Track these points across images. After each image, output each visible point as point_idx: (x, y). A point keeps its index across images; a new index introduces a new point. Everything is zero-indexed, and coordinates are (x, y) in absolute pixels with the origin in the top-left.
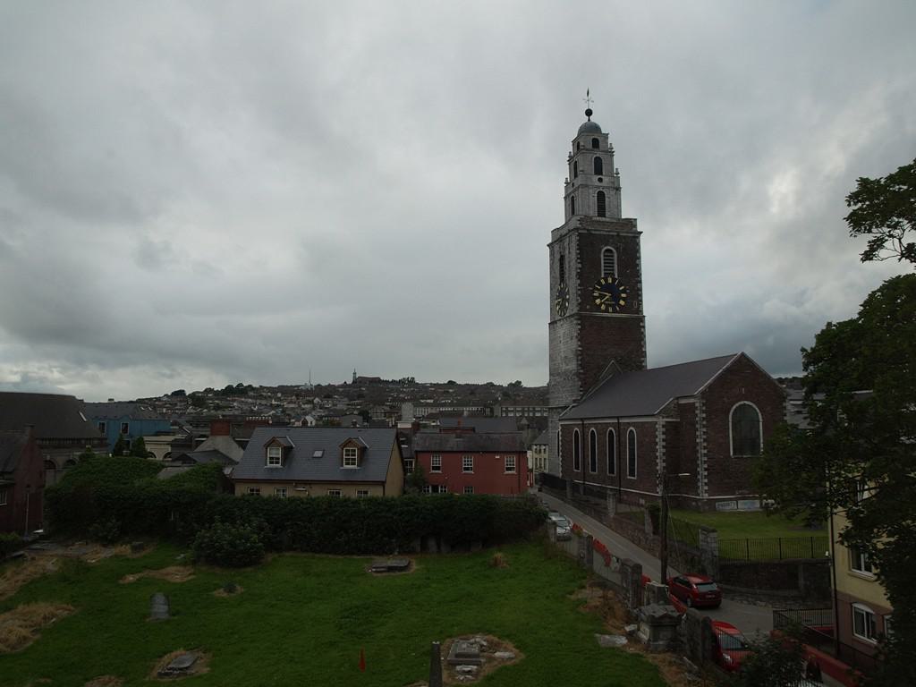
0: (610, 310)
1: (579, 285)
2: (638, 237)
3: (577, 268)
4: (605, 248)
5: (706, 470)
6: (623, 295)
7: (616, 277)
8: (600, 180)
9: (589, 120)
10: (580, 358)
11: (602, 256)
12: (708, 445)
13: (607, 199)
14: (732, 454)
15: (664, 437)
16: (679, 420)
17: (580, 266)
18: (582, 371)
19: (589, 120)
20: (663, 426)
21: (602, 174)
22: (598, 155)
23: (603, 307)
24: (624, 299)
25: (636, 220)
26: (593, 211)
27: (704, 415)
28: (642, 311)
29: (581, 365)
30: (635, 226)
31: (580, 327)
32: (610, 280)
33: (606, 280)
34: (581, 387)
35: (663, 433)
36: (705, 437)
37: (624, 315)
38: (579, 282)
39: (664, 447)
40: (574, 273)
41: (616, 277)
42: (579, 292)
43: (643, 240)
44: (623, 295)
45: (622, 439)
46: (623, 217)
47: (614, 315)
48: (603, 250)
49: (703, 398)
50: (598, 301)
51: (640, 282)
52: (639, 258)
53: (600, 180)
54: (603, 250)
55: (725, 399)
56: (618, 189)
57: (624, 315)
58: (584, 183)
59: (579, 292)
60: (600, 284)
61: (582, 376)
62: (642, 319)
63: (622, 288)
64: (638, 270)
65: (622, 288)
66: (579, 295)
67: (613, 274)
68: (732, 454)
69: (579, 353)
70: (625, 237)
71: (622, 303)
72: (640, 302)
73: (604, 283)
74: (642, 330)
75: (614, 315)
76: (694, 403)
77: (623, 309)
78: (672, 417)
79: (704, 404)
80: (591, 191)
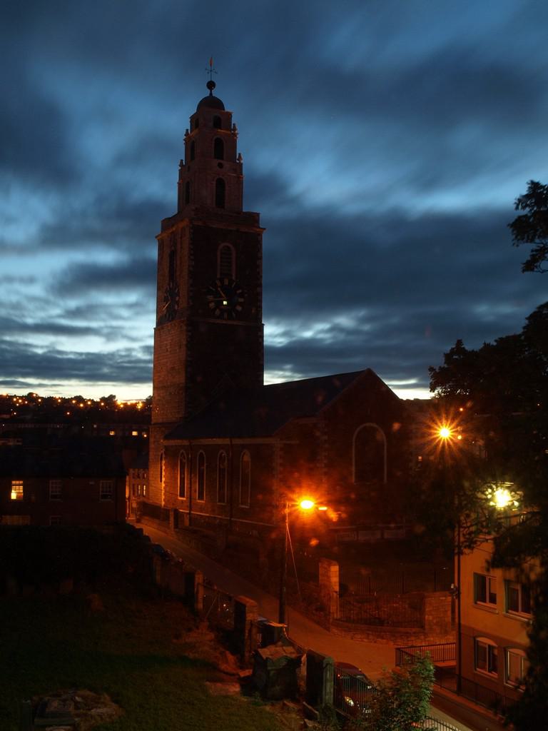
0: (226, 316)
6: (241, 300)
7: (234, 278)
9: (211, 94)
11: (219, 253)
19: (211, 94)
24: (241, 304)
31: (190, 334)
32: (226, 282)
41: (234, 278)
44: (241, 300)
46: (244, 211)
47: (230, 322)
53: (221, 165)
63: (240, 291)
65: (240, 291)
71: (239, 308)
73: (218, 283)
75: (230, 322)
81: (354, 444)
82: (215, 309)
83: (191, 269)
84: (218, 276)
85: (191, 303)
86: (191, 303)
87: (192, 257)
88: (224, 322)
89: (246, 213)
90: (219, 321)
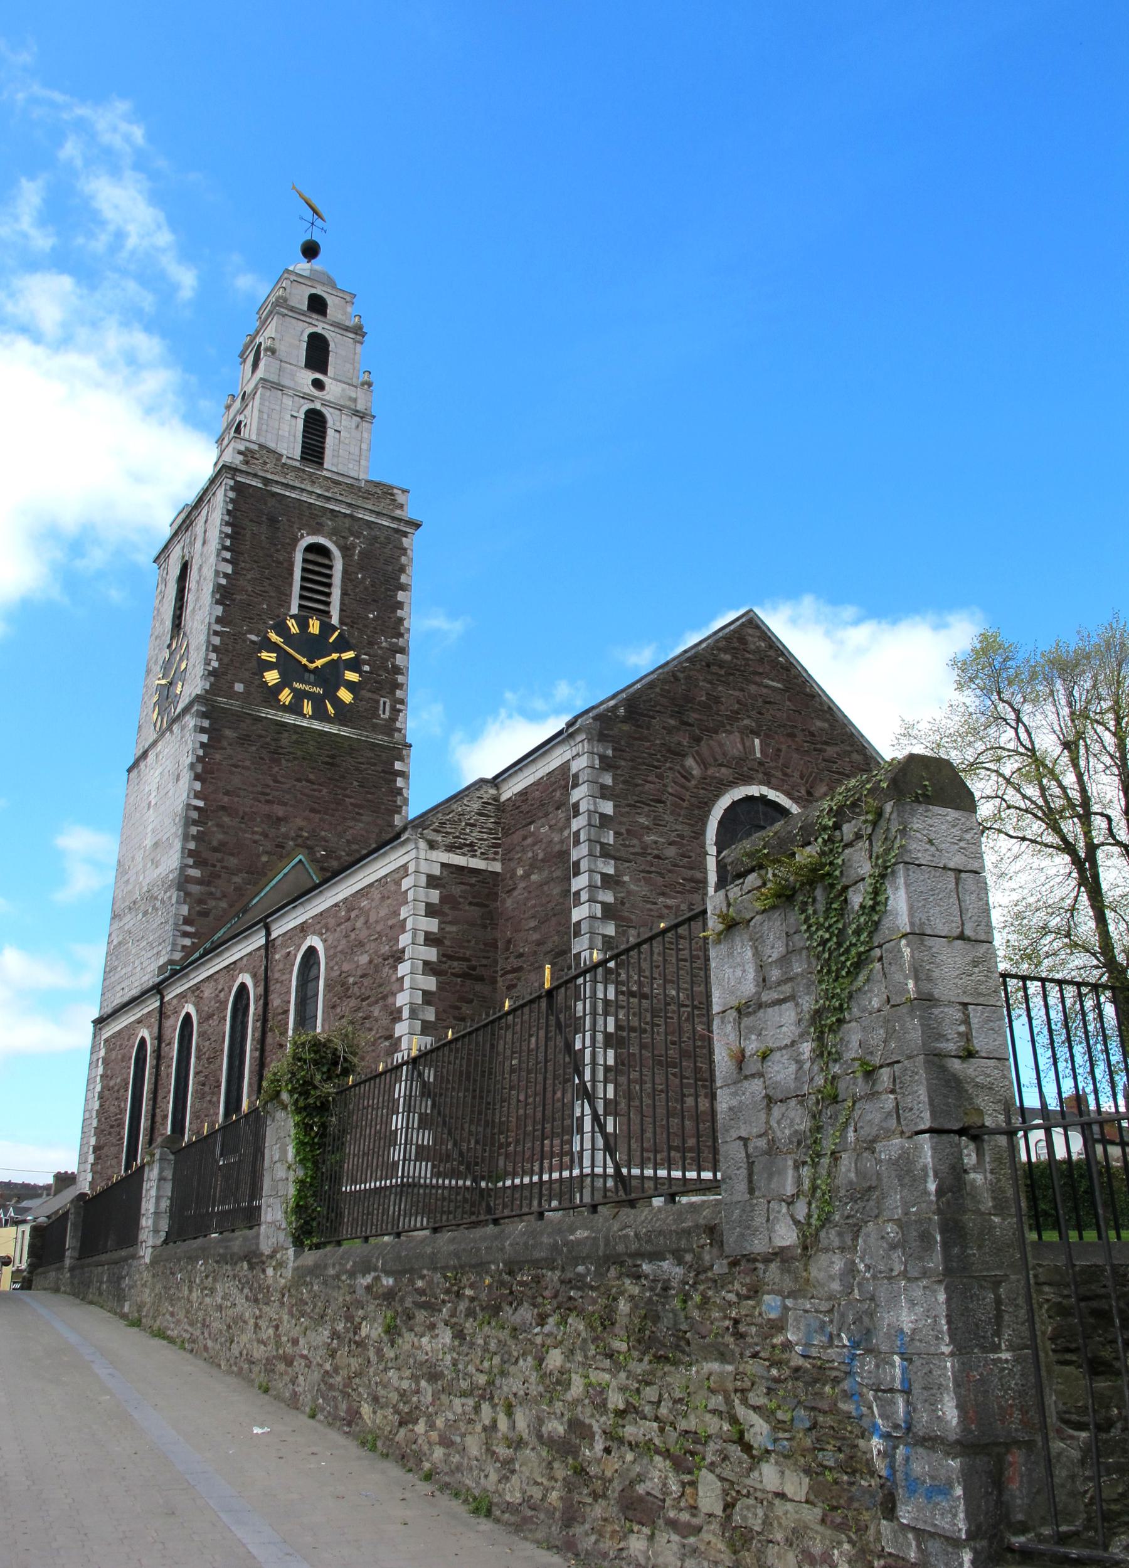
0: (308, 708)
1: (219, 620)
3: (217, 573)
5: (610, 1041)
6: (352, 676)
7: (335, 621)
10: (194, 830)
11: (299, 557)
13: (330, 433)
15: (432, 925)
16: (497, 867)
18: (195, 873)
20: (432, 882)
21: (324, 371)
22: (319, 330)
23: (286, 696)
24: (351, 686)
26: (290, 444)
27: (607, 807)
29: (191, 853)
31: (204, 738)
32: (314, 627)
33: (303, 624)
34: (187, 921)
35: (431, 911)
36: (608, 897)
37: (345, 732)
38: (219, 610)
39: (429, 968)
40: (208, 588)
41: (335, 621)
42: (217, 641)
43: (415, 543)
45: (276, 1002)
47: (317, 725)
49: (602, 737)
50: (272, 677)
51: (403, 651)
53: (318, 384)
55: (690, 762)
57: (345, 732)
58: (273, 378)
59: (217, 641)
60: (282, 630)
61: (195, 889)
62: (400, 750)
64: (401, 620)
66: (215, 649)
67: (327, 613)
69: (195, 815)
71: (345, 695)
73: (294, 629)
74: (400, 782)
75: (317, 725)
76: (565, 766)
77: (344, 714)
78: (470, 849)
79: (606, 764)
80: (288, 402)
81: (712, 850)
82: (278, 688)
83: (223, 582)
84: (294, 610)
85: (215, 664)
86: (215, 664)
87: (228, 555)
88: (305, 723)
89: (377, 484)
90: (289, 719)
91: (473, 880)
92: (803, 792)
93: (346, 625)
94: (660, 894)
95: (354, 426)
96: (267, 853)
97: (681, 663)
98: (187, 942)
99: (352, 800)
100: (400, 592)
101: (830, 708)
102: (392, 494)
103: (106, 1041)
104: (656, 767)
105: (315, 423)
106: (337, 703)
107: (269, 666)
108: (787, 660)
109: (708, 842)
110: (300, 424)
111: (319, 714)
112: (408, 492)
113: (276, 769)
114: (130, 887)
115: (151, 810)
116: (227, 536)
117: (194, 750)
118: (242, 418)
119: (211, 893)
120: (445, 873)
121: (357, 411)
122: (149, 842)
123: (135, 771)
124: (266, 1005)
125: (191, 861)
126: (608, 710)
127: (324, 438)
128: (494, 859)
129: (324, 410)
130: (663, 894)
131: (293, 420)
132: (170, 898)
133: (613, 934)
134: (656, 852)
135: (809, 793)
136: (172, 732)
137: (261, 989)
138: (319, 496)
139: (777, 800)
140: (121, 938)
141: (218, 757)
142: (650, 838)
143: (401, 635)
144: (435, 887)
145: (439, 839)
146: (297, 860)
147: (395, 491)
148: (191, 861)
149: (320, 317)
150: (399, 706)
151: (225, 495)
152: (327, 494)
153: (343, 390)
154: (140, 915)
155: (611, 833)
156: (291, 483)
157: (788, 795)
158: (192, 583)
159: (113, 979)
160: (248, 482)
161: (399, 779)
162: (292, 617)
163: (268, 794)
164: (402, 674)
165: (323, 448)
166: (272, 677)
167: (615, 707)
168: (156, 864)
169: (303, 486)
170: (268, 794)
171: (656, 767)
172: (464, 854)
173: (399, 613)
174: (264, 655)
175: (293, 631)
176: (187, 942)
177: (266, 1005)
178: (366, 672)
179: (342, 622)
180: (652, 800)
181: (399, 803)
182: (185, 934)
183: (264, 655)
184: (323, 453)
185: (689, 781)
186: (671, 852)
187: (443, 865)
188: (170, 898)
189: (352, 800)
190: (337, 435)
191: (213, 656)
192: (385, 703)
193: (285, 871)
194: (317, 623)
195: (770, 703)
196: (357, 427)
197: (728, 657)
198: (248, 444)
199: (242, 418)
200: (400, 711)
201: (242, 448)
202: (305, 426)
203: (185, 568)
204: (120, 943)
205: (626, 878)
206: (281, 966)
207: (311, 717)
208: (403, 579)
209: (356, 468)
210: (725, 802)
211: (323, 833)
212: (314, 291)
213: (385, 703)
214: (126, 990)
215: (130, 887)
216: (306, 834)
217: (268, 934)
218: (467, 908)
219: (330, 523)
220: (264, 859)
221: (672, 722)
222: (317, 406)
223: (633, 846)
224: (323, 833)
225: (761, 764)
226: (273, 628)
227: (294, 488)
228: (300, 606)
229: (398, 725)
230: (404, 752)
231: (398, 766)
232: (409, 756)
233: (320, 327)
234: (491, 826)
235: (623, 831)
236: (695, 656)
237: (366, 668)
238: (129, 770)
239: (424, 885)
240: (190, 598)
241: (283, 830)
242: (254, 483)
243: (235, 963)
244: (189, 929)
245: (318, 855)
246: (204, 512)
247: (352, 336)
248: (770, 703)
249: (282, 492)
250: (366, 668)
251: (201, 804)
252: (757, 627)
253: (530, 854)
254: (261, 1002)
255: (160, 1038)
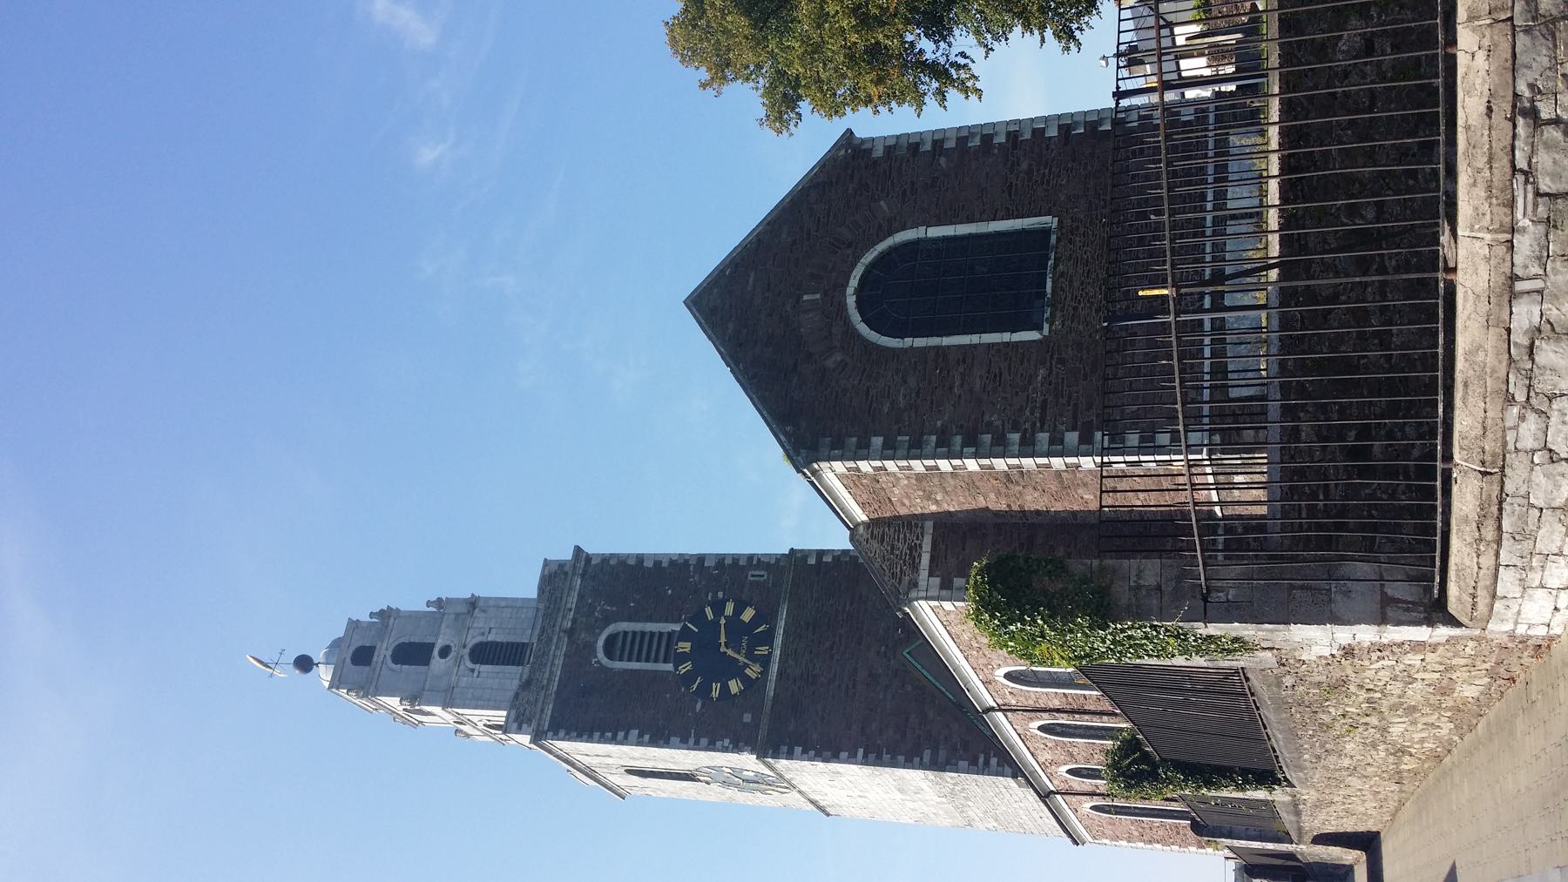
2: (589, 558)
4: (601, 655)
6: (729, 609)
7: (677, 627)
8: (445, 652)
12: (989, 428)
13: (491, 638)
14: (1033, 335)
17: (634, 733)
18: (927, 755)
23: (753, 671)
24: (738, 611)
25: (546, 563)
28: (780, 558)
30: (561, 565)
32: (685, 647)
41: (677, 627)
42: (704, 741)
44: (729, 609)
47: (778, 641)
48: (605, 661)
51: (701, 558)
52: (640, 558)
53: (445, 652)
54: (605, 661)
55: (830, 363)
56: (473, 603)
60: (688, 679)
61: (942, 754)
62: (796, 558)
67: (671, 634)
68: (1033, 335)
70: (581, 597)
71: (748, 615)
72: (754, 562)
73: (686, 667)
75: (778, 641)
78: (915, 549)
82: (746, 680)
83: (647, 737)
84: (670, 667)
85: (726, 742)
86: (726, 742)
87: (621, 735)
88: (777, 652)
89: (541, 590)
91: (942, 547)
92: (849, 251)
93: (681, 617)
94: (951, 392)
95: (483, 615)
96: (903, 686)
97: (740, 370)
98: (994, 761)
99: (848, 605)
100: (645, 564)
101: (768, 224)
102: (550, 576)
103: (1094, 838)
104: (837, 395)
105: (485, 653)
106: (755, 621)
107: (725, 689)
108: (726, 267)
109: (901, 345)
110: (485, 668)
111: (768, 638)
112: (546, 560)
113: (823, 679)
114: (941, 812)
115: (867, 795)
116: (602, 736)
117: (810, 760)
118: (480, 725)
119: (946, 738)
120: (937, 573)
121: (469, 612)
122: (899, 796)
123: (828, 809)
124: (1058, 711)
125: (917, 760)
126: (789, 441)
127: (497, 643)
128: (922, 527)
129: (470, 646)
130: (951, 388)
131: (483, 675)
132: (951, 778)
133: (990, 436)
134: (913, 395)
135: (849, 246)
136: (792, 779)
137: (1045, 715)
138: (557, 648)
139: (858, 278)
140: (991, 820)
141: (815, 736)
142: (902, 402)
143: (686, 561)
144: (951, 582)
145: (907, 578)
146: (908, 656)
147: (546, 572)
148: (917, 760)
149: (376, 654)
150: (755, 562)
151: (563, 740)
152: (555, 641)
153: (447, 627)
154: (970, 803)
155: (899, 438)
156: (547, 675)
157: (853, 266)
158: (648, 765)
159: (1031, 826)
160: (548, 718)
161: (825, 559)
162: (676, 669)
163: (848, 688)
164: (724, 559)
165: (508, 643)
166: (734, 686)
167: (786, 434)
168: (918, 791)
169: (549, 664)
170: (847, 685)
171: (837, 395)
172: (920, 556)
173: (665, 564)
174: (715, 694)
175: (688, 668)
176: (994, 761)
177: (1058, 711)
178: (724, 595)
179: (677, 621)
180: (867, 399)
181: (848, 559)
182: (987, 763)
183: (715, 694)
184: (513, 644)
185: (847, 364)
186: (912, 381)
187: (930, 575)
188: (951, 778)
189: (848, 605)
190: (494, 631)
191: (719, 744)
192: (753, 576)
193: (919, 667)
194: (681, 644)
195: (769, 285)
196: (484, 611)
197: (731, 325)
198: (511, 720)
199: (480, 725)
200: (759, 560)
201: (515, 725)
202: (487, 664)
203: (631, 772)
204: (996, 820)
205: (939, 423)
206: (1022, 699)
207: (771, 647)
208: (632, 562)
209: (525, 610)
210: (863, 329)
211: (881, 632)
212: (348, 661)
213: (753, 576)
214: (1042, 815)
215: (941, 812)
216: (883, 648)
217: (992, 709)
218: (967, 551)
219: (583, 635)
220: (909, 688)
221: (795, 380)
222: (467, 651)
223: (910, 417)
224: (881, 632)
225: (825, 294)
226: (688, 688)
227: (551, 673)
228: (665, 661)
229: (773, 562)
230: (799, 555)
231: (812, 561)
232: (802, 551)
233: (384, 651)
234: (892, 530)
235: (896, 427)
236: (732, 357)
237: (720, 594)
238: (828, 815)
239: (950, 592)
240: (661, 766)
241: (880, 671)
242: (549, 712)
243: (1019, 735)
244: (981, 760)
245: (903, 636)
246: (578, 757)
247: (392, 621)
248: (769, 285)
249: (556, 684)
250: (720, 594)
251: (861, 751)
252: (699, 296)
253: (918, 500)
254: (1057, 715)
255: (1092, 794)
